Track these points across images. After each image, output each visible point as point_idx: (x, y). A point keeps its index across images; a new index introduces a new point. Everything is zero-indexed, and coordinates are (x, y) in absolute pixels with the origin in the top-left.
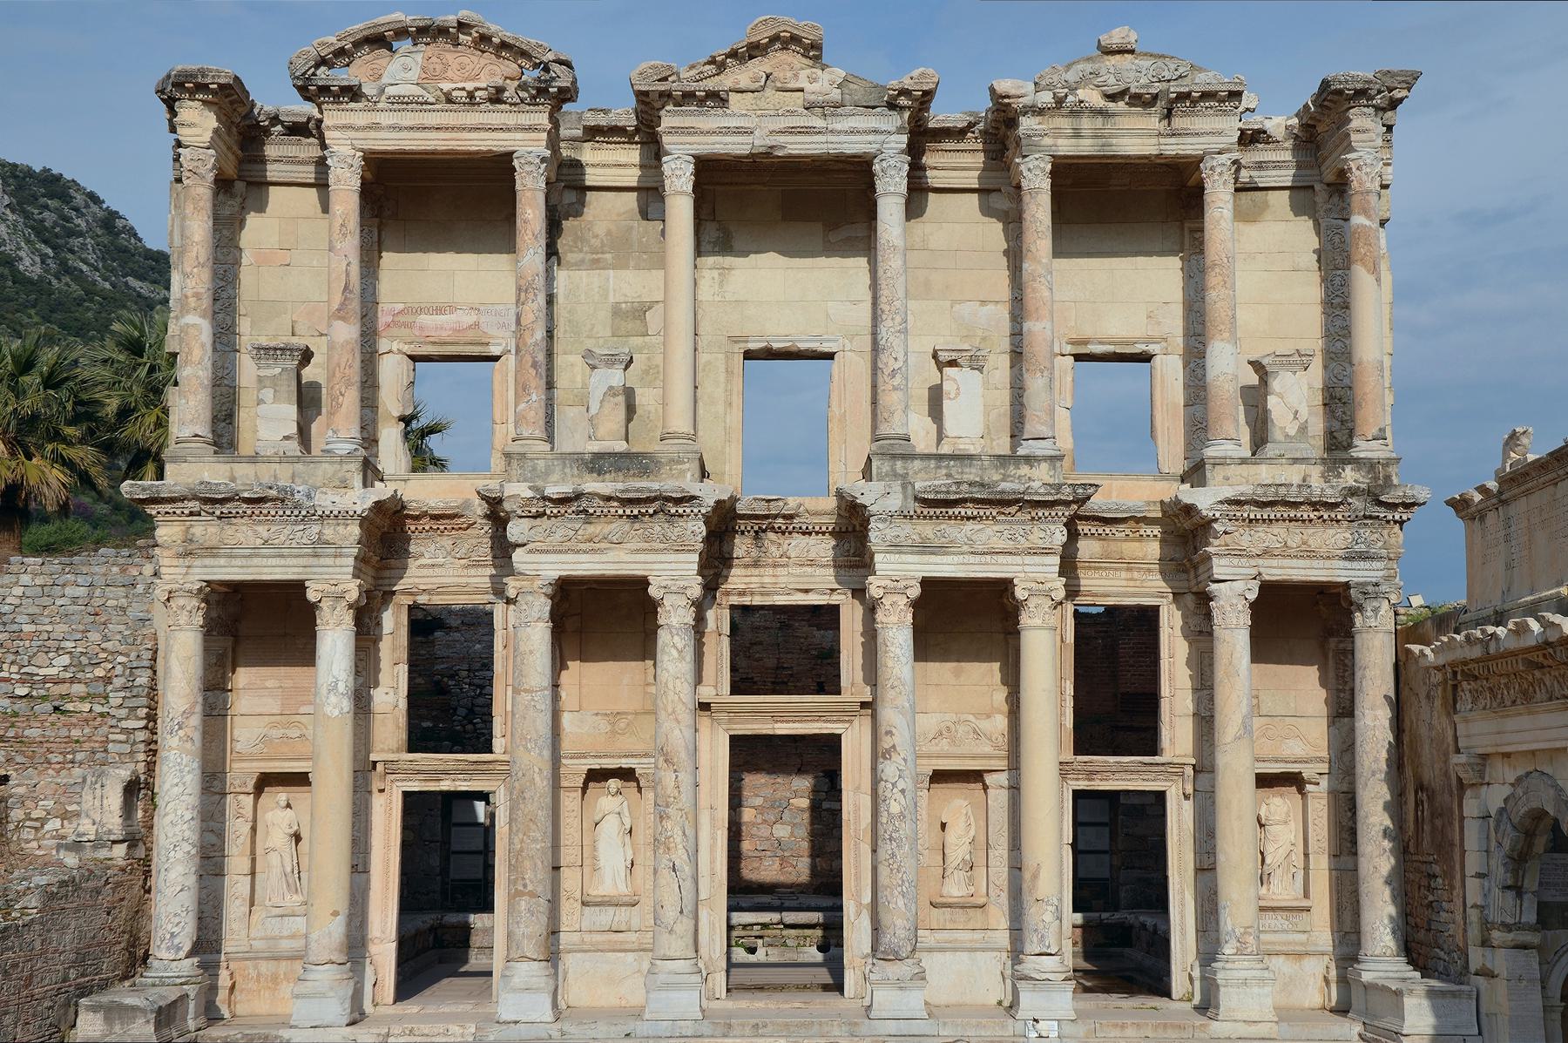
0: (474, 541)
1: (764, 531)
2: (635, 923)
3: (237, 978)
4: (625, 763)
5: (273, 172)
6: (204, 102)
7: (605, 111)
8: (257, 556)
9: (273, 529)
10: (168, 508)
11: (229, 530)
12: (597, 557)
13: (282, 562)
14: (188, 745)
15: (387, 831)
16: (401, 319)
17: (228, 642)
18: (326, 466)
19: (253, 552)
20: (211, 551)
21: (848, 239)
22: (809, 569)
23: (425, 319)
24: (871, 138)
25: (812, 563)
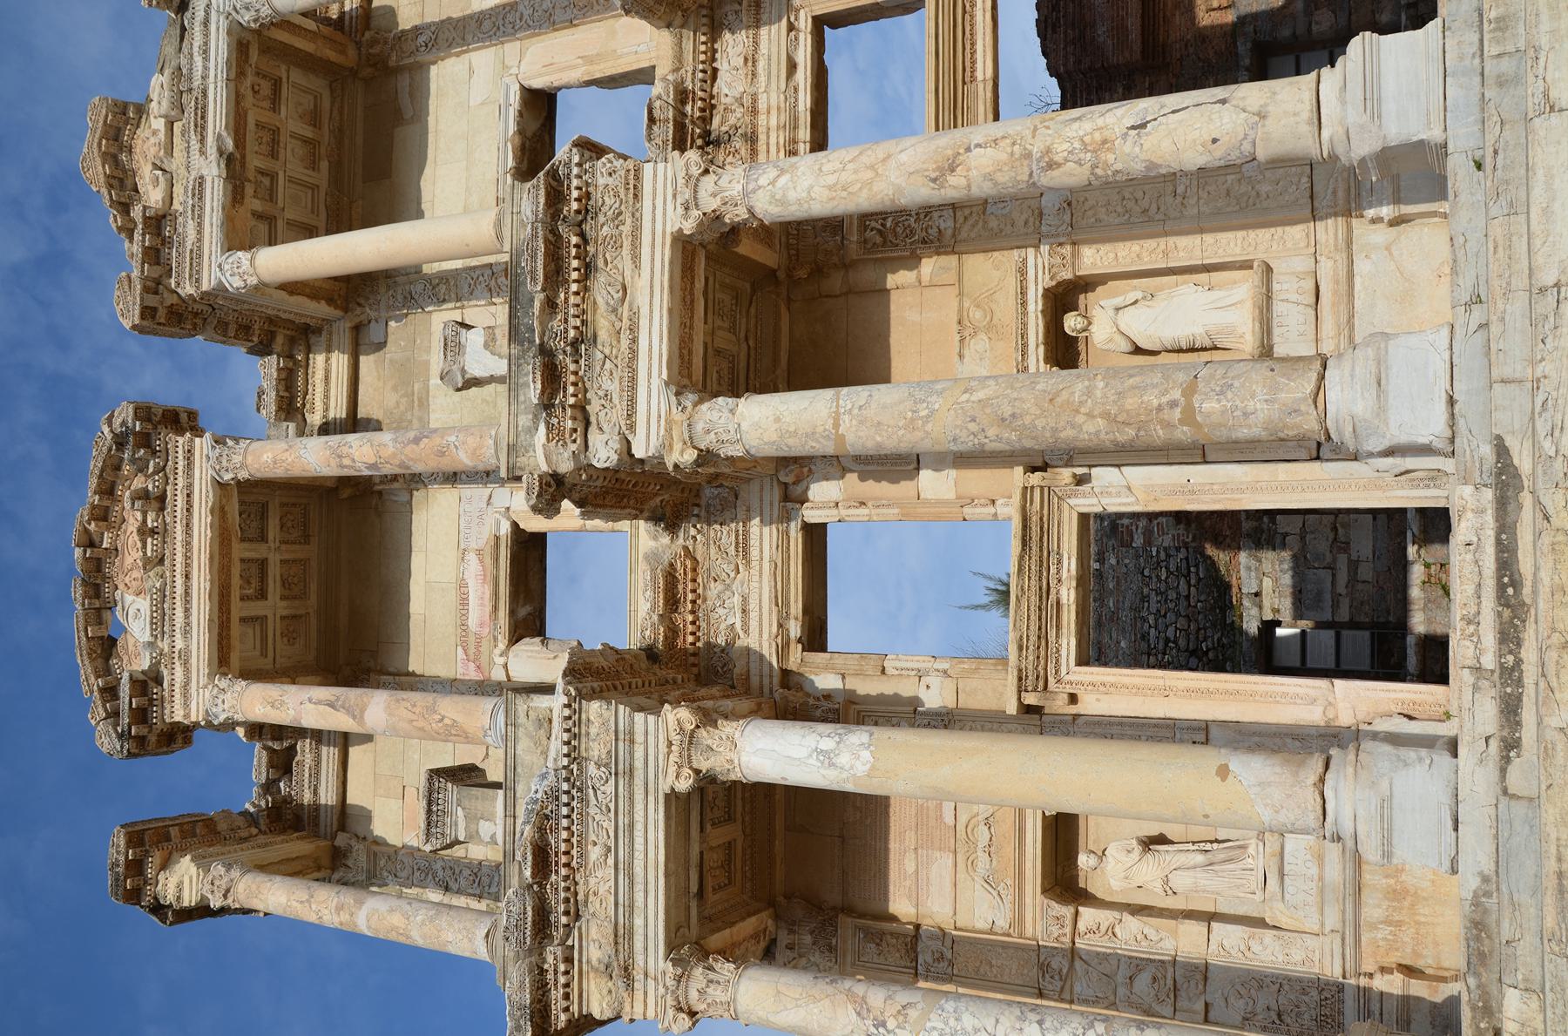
0: (713, 550)
1: (709, 133)
2: (1303, 264)
3: (1392, 959)
4: (1035, 305)
5: (328, 796)
6: (164, 866)
7: (260, 394)
8: (631, 865)
9: (593, 837)
10: (556, 995)
11: (594, 905)
12: (644, 323)
13: (639, 827)
14: (913, 1014)
15: (1138, 690)
16: (472, 650)
17: (846, 923)
18: (519, 747)
19: (629, 874)
20: (622, 936)
21: (411, 95)
22: (761, 64)
23: (473, 622)
24: (213, 28)
25: (751, 60)
